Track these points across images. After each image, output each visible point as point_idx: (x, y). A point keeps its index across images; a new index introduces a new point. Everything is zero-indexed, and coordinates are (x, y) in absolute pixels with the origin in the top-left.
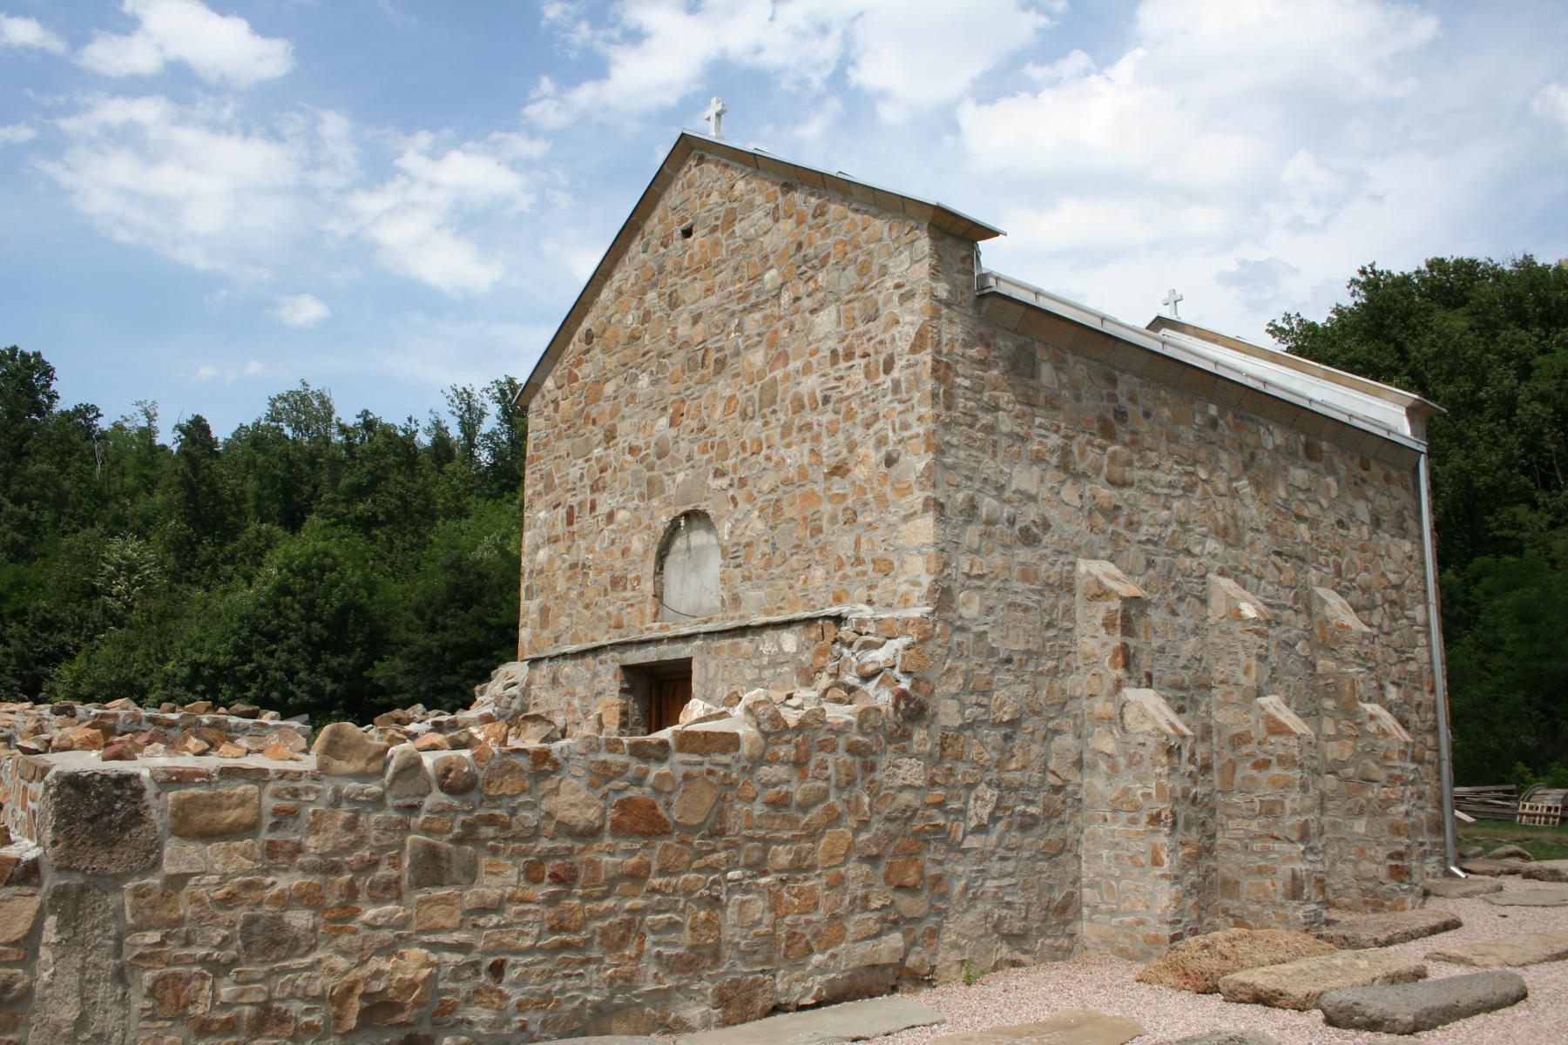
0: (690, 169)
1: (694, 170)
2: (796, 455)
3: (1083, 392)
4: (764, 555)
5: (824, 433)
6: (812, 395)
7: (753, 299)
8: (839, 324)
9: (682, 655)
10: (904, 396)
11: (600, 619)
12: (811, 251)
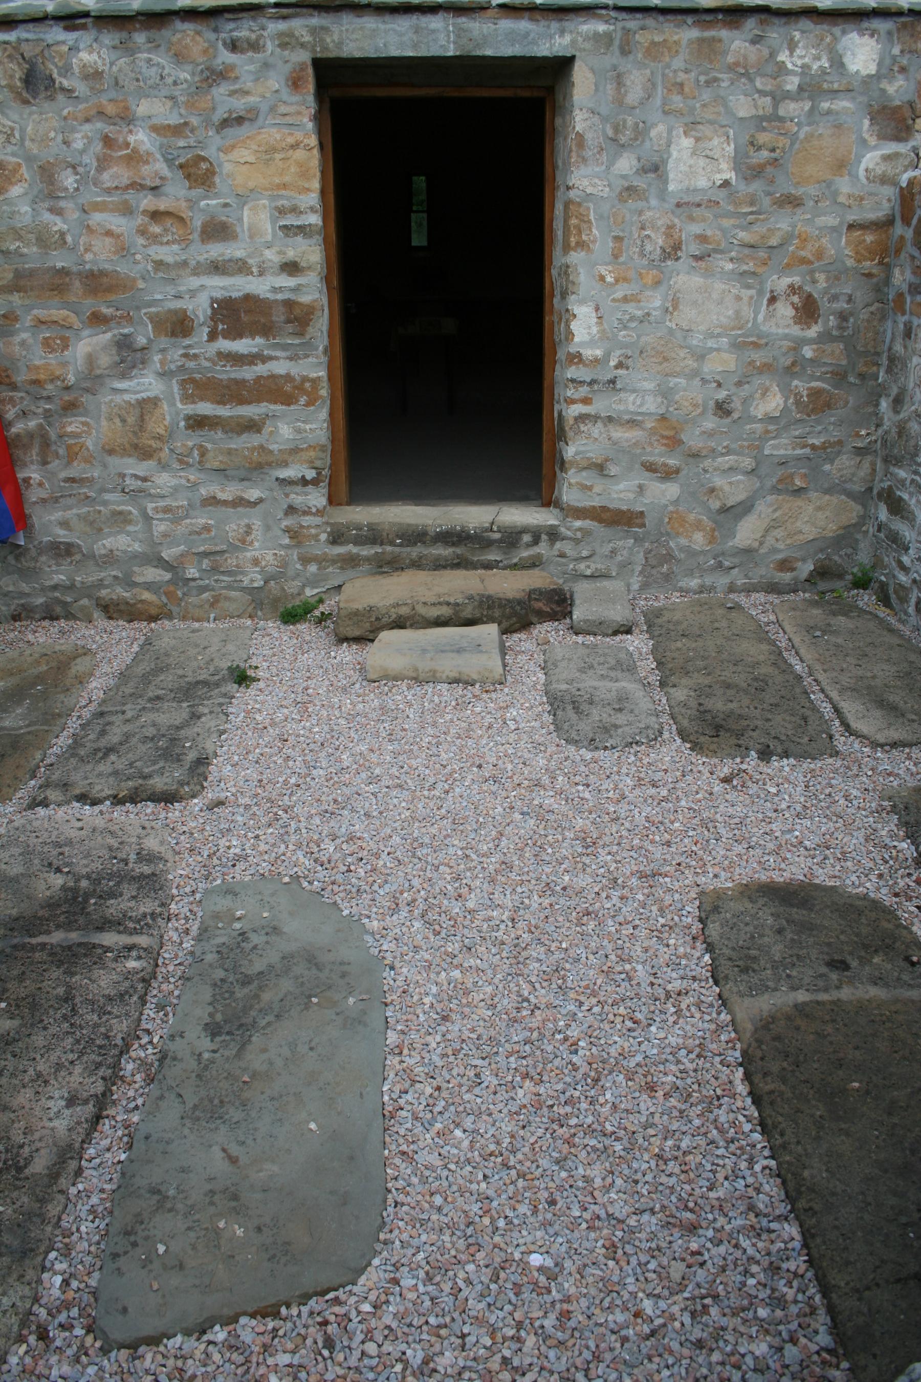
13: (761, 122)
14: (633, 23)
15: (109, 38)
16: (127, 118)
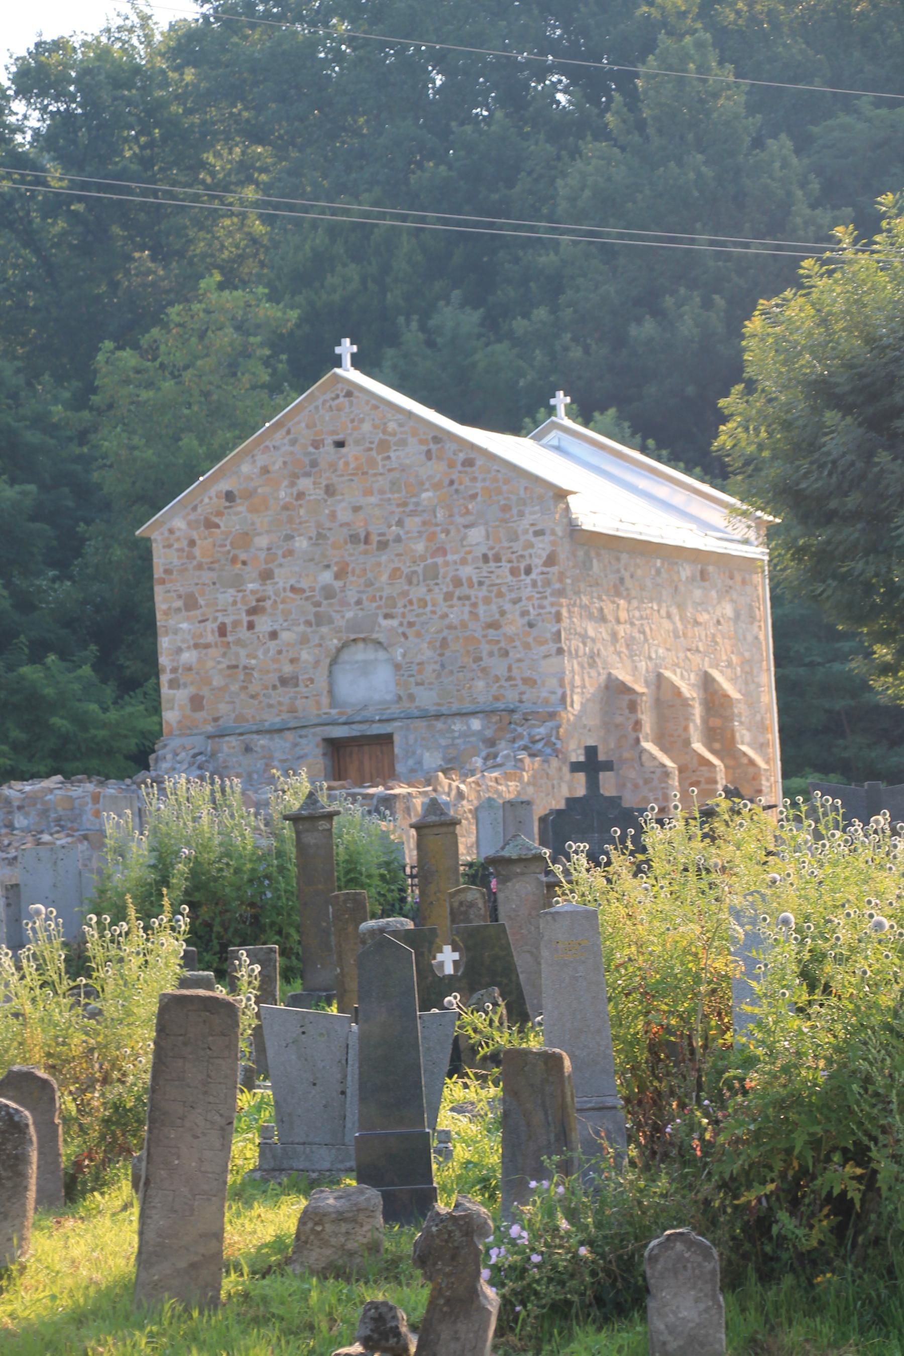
0: (337, 396)
1: (341, 399)
2: (457, 613)
3: (239, 293)
4: (434, 671)
5: (480, 603)
6: (470, 579)
7: (411, 507)
8: (488, 538)
9: (382, 731)
10: (541, 590)
11: (270, 706)
12: (462, 488)
13: (447, 747)
14: (409, 721)
15: (268, 736)
16: (271, 758)
